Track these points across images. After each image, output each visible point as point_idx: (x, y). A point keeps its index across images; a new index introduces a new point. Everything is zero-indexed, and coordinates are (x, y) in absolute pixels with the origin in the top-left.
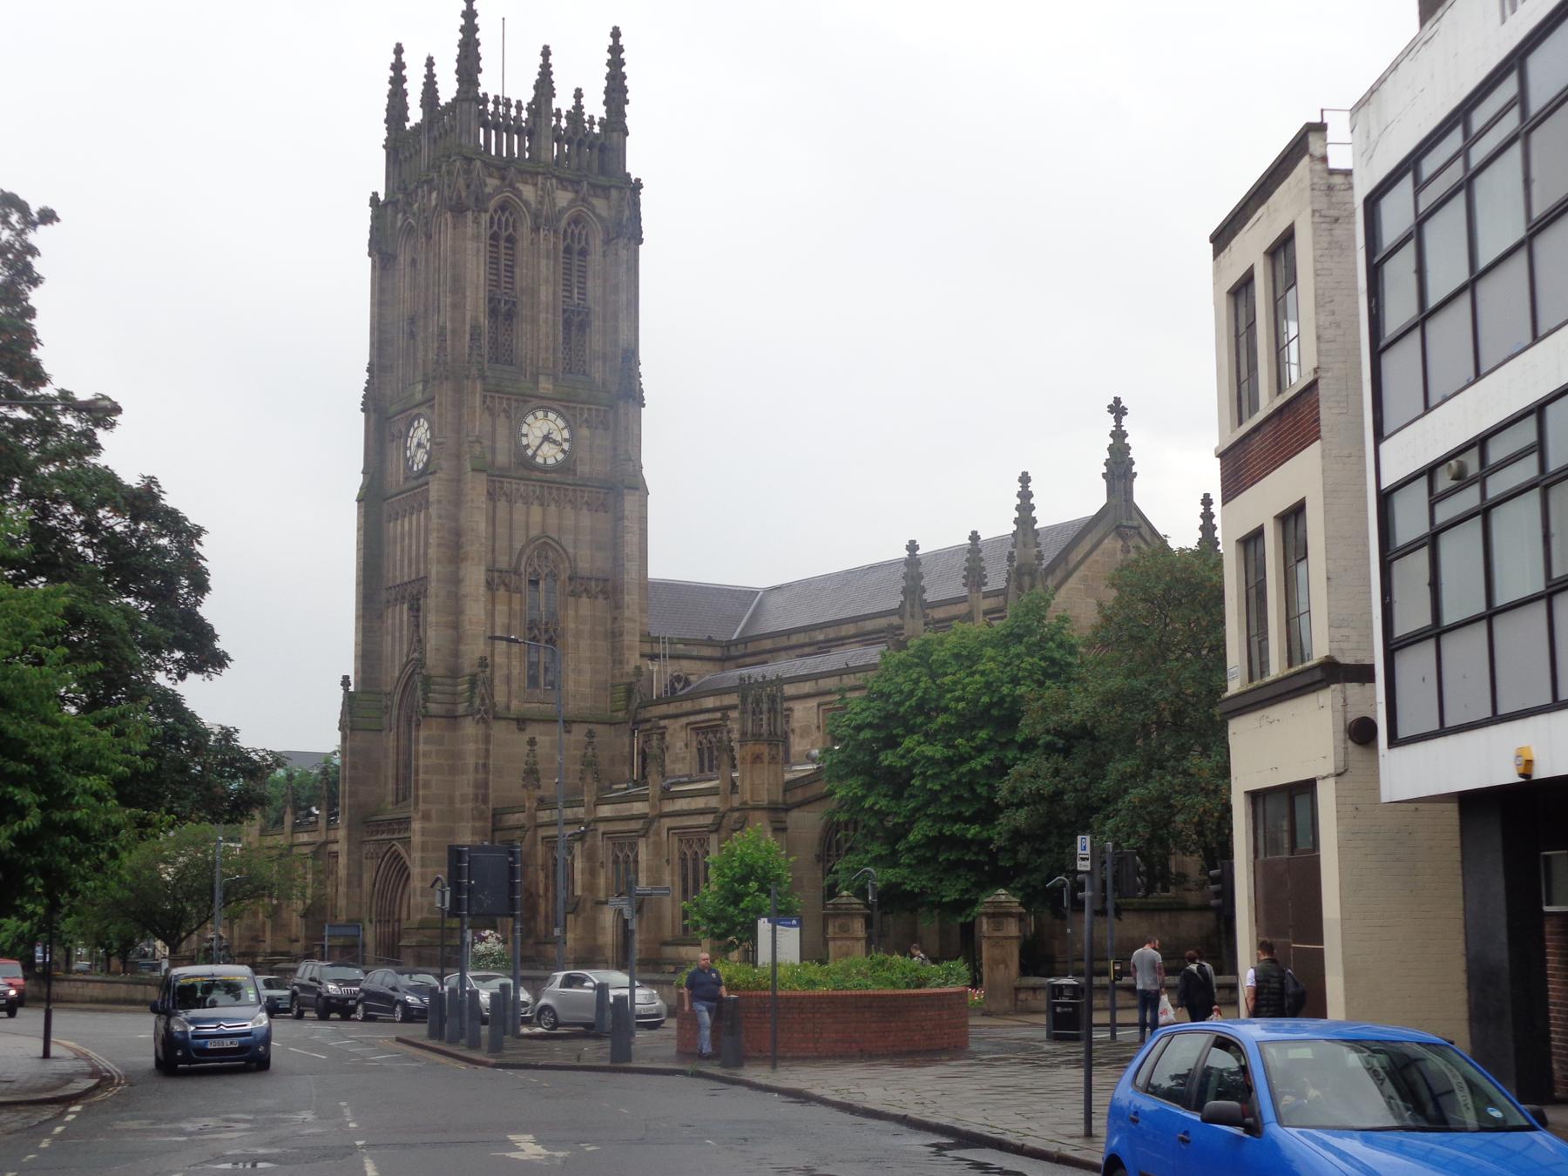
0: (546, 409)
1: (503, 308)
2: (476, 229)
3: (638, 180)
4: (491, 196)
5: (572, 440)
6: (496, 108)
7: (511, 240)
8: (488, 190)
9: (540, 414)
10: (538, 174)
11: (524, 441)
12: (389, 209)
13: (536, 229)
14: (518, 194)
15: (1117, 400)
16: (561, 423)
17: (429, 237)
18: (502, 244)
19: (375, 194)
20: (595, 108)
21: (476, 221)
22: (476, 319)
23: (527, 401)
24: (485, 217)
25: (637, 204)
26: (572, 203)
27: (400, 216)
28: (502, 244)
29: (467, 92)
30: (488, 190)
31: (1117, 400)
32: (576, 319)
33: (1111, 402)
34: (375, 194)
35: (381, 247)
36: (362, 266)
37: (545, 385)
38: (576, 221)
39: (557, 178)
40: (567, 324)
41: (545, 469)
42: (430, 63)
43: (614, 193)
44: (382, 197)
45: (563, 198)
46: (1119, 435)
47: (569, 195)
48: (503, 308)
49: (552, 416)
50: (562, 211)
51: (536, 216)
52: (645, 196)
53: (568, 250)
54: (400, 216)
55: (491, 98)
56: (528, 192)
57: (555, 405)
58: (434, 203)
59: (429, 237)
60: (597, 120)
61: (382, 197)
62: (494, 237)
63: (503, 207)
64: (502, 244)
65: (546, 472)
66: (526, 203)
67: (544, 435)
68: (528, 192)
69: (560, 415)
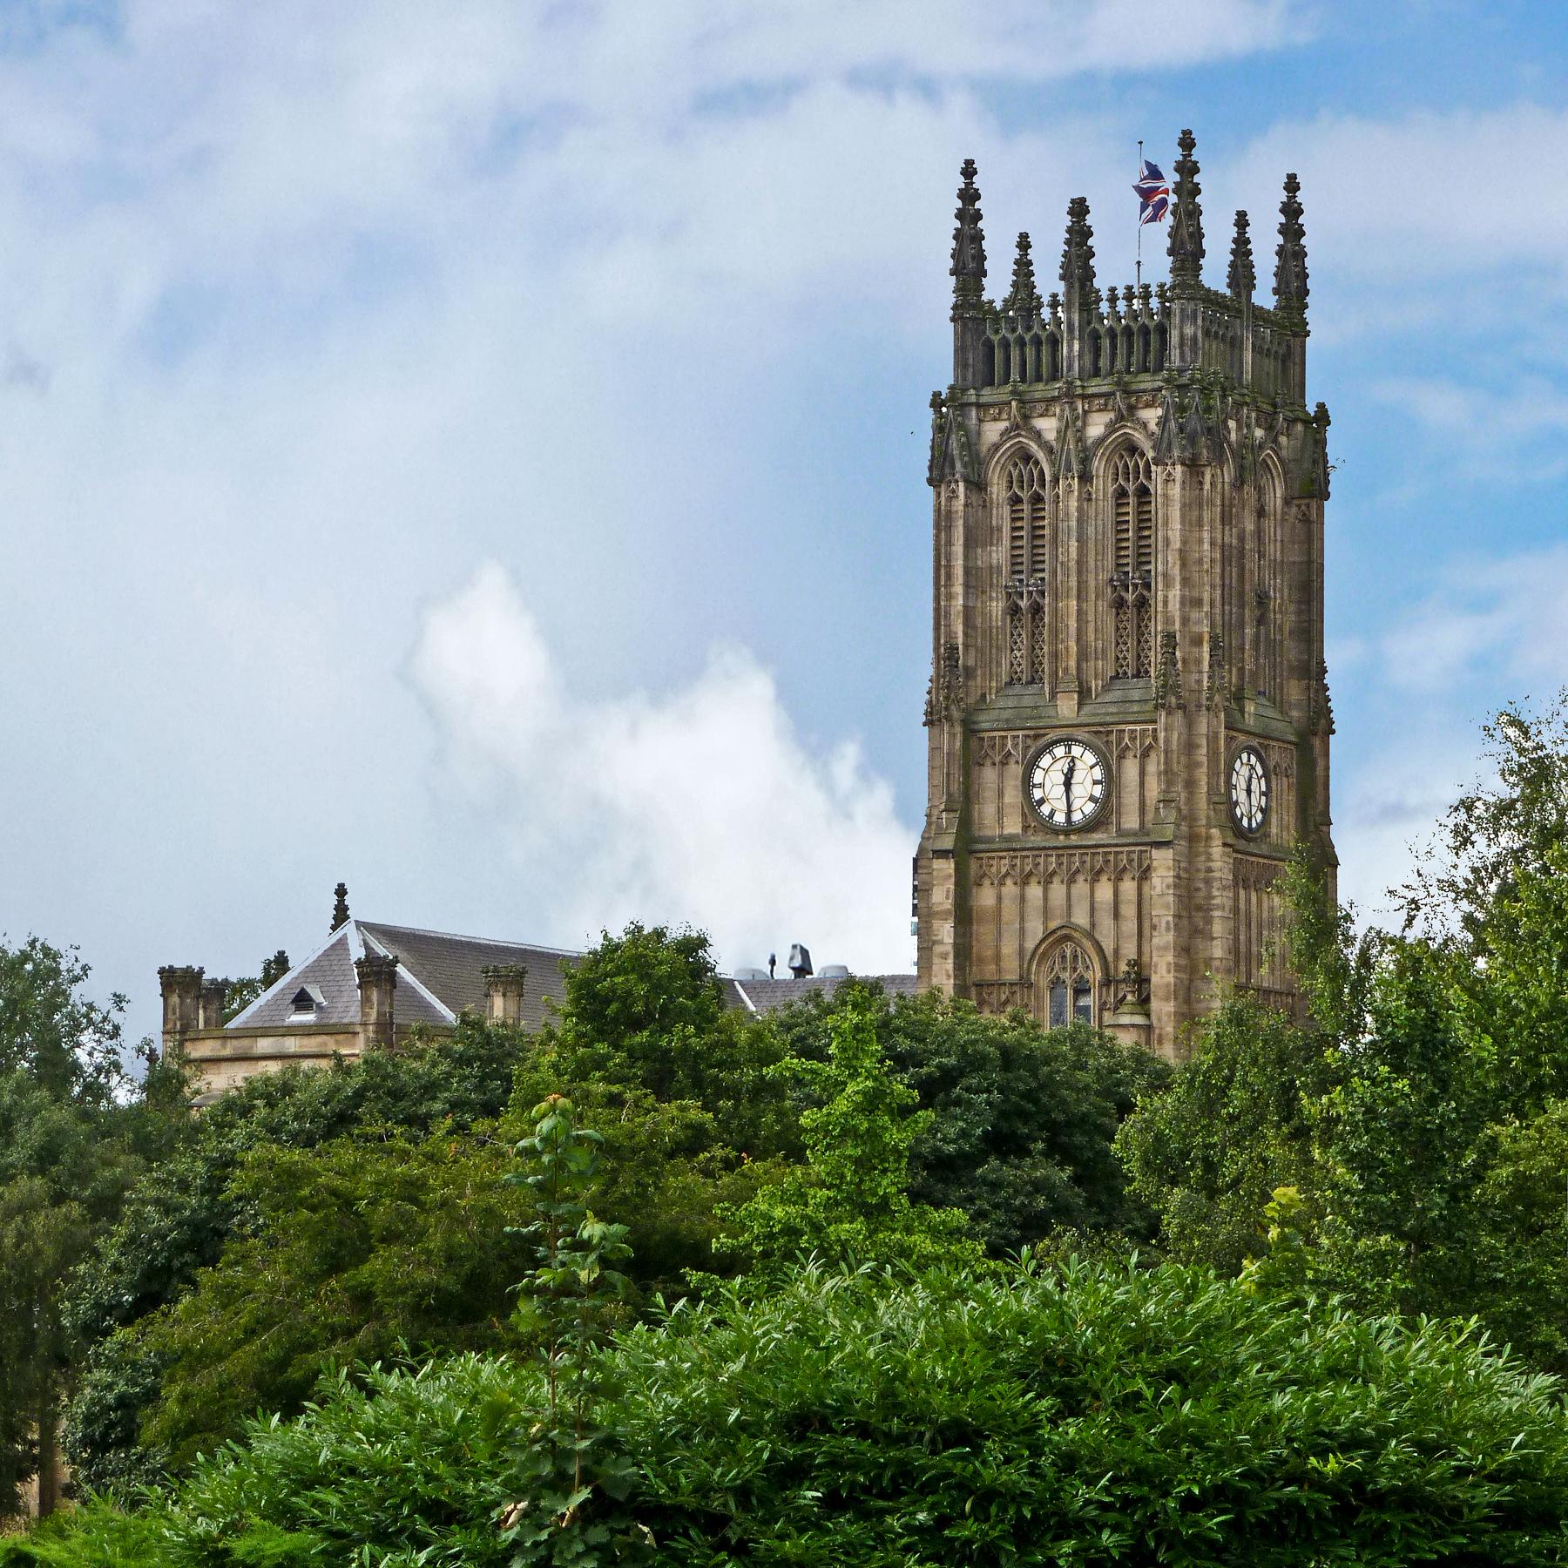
0: (1068, 741)
5: (1111, 781)
7: (1037, 499)
11: (1037, 794)
13: (1056, 480)
14: (1038, 436)
26: (1111, 428)
32: (1130, 597)
37: (1067, 707)
40: (1120, 604)
53: (1121, 494)
56: (1048, 426)
57: (1081, 734)
60: (1154, 289)
67: (1068, 784)
69: (1087, 745)
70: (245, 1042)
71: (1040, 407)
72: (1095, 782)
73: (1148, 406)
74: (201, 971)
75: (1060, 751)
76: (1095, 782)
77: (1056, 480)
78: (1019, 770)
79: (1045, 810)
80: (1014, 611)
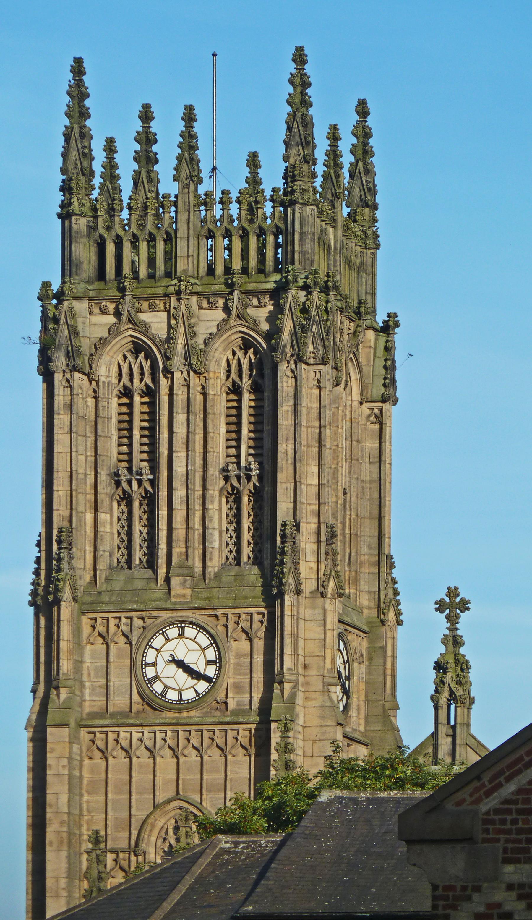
0: (182, 624)
9: (173, 632)
10: (167, 296)
11: (150, 672)
15: (452, 592)
16: (204, 640)
23: (155, 617)
31: (452, 592)
33: (442, 595)
39: (198, 294)
41: (181, 706)
42: (189, 117)
46: (454, 641)
49: (190, 632)
65: (180, 711)
79: (158, 687)
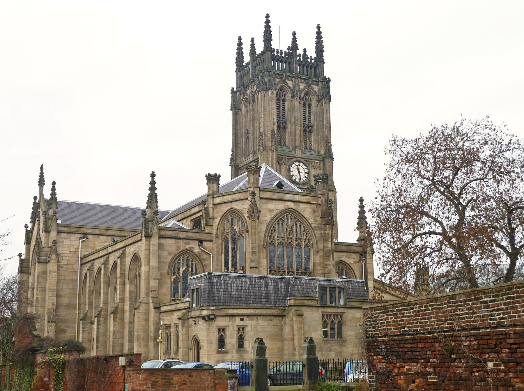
0: (299, 161)
1: (282, 125)
2: (272, 94)
3: (329, 78)
4: (278, 84)
6: (278, 54)
7: (284, 101)
8: (276, 82)
11: (292, 173)
12: (238, 93)
13: (293, 97)
17: (254, 101)
18: (281, 101)
19: (233, 88)
20: (312, 53)
21: (272, 94)
22: (273, 129)
24: (275, 92)
25: (329, 87)
27: (242, 95)
28: (281, 102)
29: (267, 48)
30: (276, 82)
32: (308, 129)
34: (233, 88)
35: (235, 107)
36: (229, 115)
37: (298, 153)
38: (307, 94)
40: (305, 131)
43: (320, 83)
44: (235, 89)
45: (302, 86)
47: (305, 85)
48: (282, 125)
50: (301, 91)
51: (293, 92)
52: (331, 84)
53: (304, 104)
54: (242, 95)
55: (276, 50)
56: (290, 83)
58: (255, 89)
59: (254, 101)
61: (235, 89)
62: (278, 99)
63: (281, 89)
64: (281, 102)
66: (289, 87)
68: (290, 83)
70: (281, 195)
71: (289, 78)
72: (306, 173)
73: (314, 85)
74: (216, 173)
75: (297, 164)
76: (306, 173)
77: (293, 97)
78: (287, 167)
80: (279, 127)
